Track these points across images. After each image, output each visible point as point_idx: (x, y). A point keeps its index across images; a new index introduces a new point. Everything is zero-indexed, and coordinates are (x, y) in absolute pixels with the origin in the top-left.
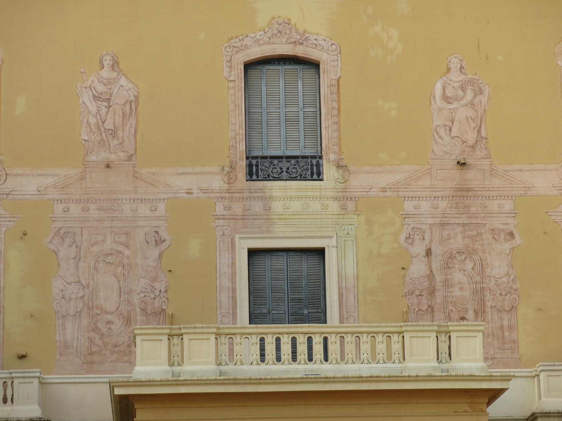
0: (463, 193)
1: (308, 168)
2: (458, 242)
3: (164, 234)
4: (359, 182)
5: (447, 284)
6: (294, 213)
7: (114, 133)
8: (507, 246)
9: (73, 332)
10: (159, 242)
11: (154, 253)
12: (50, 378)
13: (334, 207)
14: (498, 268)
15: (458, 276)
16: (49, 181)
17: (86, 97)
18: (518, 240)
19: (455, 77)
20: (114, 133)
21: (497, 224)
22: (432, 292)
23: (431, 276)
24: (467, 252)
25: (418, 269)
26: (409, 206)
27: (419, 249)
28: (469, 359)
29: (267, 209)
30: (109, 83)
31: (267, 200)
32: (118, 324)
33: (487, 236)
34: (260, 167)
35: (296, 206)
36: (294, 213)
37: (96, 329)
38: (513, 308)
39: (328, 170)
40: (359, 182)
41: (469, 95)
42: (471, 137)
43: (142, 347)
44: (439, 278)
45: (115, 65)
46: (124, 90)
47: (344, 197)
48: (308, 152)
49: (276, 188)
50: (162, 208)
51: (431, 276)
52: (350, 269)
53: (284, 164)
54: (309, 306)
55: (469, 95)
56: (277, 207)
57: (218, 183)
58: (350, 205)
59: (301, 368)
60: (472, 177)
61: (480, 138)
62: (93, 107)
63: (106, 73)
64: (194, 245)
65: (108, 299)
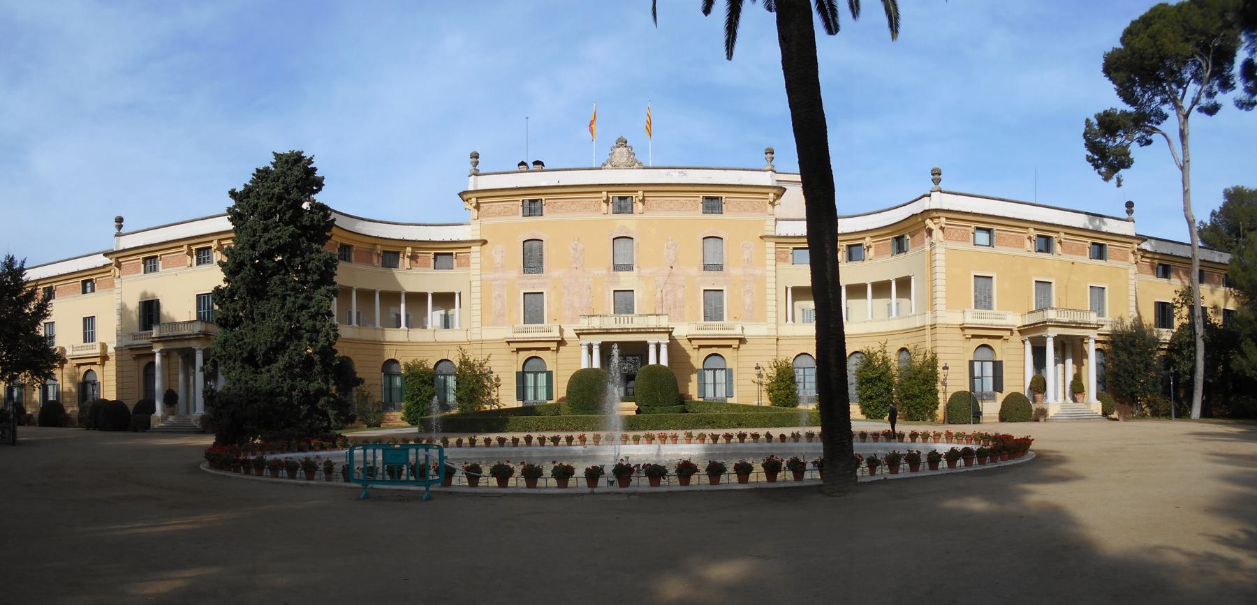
0: (670, 275)
6: (626, 280)
14: (680, 295)
25: (659, 295)
34: (616, 268)
36: (626, 280)
47: (639, 276)
57: (605, 272)
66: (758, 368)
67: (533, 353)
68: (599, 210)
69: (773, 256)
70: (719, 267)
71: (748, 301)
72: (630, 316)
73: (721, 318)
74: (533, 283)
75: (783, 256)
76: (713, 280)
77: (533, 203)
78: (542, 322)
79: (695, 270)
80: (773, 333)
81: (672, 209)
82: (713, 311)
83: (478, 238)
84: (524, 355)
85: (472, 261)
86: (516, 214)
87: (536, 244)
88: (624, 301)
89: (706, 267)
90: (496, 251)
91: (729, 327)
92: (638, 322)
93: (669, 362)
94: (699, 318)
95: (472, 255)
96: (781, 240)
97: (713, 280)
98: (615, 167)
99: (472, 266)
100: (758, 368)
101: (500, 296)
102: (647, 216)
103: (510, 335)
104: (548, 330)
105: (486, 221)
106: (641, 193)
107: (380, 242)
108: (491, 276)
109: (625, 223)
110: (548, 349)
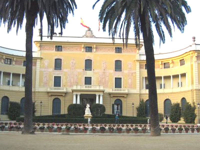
0: (104, 72)
2: (103, 77)
6: (89, 74)
8: (107, 77)
9: (69, 84)
10: (77, 76)
11: (76, 77)
12: (67, 88)
13: (93, 73)
18: (109, 77)
21: (107, 75)
23: (101, 80)
25: (100, 79)
26: (99, 73)
28: (102, 88)
30: (73, 61)
31: (87, 73)
33: (106, 77)
36: (89, 74)
38: (108, 83)
39: (92, 70)
40: (95, 71)
42: (105, 67)
43: (74, 86)
45: (74, 60)
46: (74, 62)
51: (101, 80)
56: (88, 73)
57: (82, 70)
59: (87, 89)
60: (105, 71)
61: (106, 67)
63: (73, 60)
65: (72, 81)
67: (56, 97)
69: (139, 67)
71: (130, 81)
72: (90, 85)
74: (57, 73)
75: (142, 67)
77: (59, 48)
78: (60, 86)
80: (138, 92)
81: (105, 51)
83: (40, 57)
84: (53, 98)
85: (37, 64)
87: (59, 60)
88: (88, 81)
90: (46, 62)
91: (124, 90)
92: (93, 88)
93: (103, 102)
94: (113, 87)
95: (37, 62)
96: (140, 61)
98: (87, 37)
99: (37, 66)
101: (46, 77)
103: (49, 90)
104: (63, 89)
105: (43, 51)
106: (95, 46)
107: (5, 55)
108: (43, 70)
109: (89, 56)
110: (62, 95)
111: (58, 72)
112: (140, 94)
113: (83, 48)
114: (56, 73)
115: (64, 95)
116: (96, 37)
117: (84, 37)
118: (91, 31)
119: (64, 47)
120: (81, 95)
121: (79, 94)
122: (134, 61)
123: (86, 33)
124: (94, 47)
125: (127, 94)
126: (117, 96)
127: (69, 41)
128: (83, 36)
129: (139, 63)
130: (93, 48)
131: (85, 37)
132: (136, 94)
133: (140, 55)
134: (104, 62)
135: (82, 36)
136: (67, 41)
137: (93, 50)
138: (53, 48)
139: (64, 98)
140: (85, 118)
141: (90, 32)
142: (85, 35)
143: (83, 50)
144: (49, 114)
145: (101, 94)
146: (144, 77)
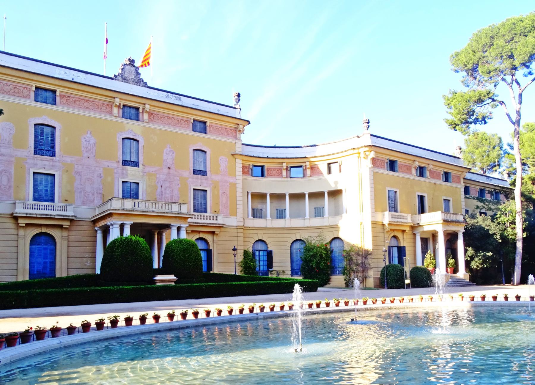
0: (169, 174)
1: (136, 164)
2: (168, 185)
3: (102, 175)
4: (147, 169)
5: (165, 193)
6: (132, 174)
7: (90, 150)
10: (101, 177)
11: (99, 179)
13: (141, 174)
15: (167, 192)
16: (74, 159)
17: (83, 140)
19: (168, 149)
20: (90, 150)
22: (162, 195)
24: (169, 187)
27: (159, 185)
29: (127, 172)
31: (127, 170)
32: (91, 195)
34: (125, 163)
35: (133, 172)
36: (132, 174)
37: (85, 196)
39: (140, 165)
40: (147, 169)
41: (171, 153)
44: (164, 192)
45: (91, 133)
47: (143, 172)
48: (136, 161)
49: (129, 168)
50: (102, 169)
51: (162, 192)
52: (145, 188)
53: (130, 163)
54: (135, 196)
55: (171, 153)
56: (129, 172)
58: (145, 174)
60: (171, 171)
61: (173, 163)
62: (85, 143)
63: (89, 135)
64: (109, 179)
65: (88, 189)
66: (234, 249)
67: (44, 230)
68: (110, 113)
70: (204, 173)
73: (205, 211)
75: (246, 170)
76: (200, 183)
79: (188, 173)
80: (242, 224)
81: (170, 124)
82: (200, 207)
86: (27, 97)
88: (131, 192)
89: (195, 172)
97: (200, 183)
98: (125, 80)
100: (234, 249)
102: (151, 125)
110: (61, 227)
111: (47, 163)
112: (245, 228)
113: (116, 106)
114: (39, 162)
115: (66, 224)
116: (149, 85)
117: (118, 80)
118: (134, 66)
119: (61, 95)
120: (135, 228)
121: (129, 222)
122: (233, 155)
123: (122, 70)
124: (143, 109)
125: (220, 227)
126: (199, 232)
127: (74, 80)
128: (115, 76)
129: (240, 161)
130: (143, 112)
131: (120, 79)
132: (237, 227)
133: (243, 144)
134: (168, 149)
135: (112, 76)
136: (71, 80)
137: (141, 115)
138: (25, 90)
139: (65, 234)
140: (158, 284)
141: (133, 69)
142: (121, 75)
143: (115, 110)
144: (20, 279)
145: (185, 225)
146: (250, 192)
